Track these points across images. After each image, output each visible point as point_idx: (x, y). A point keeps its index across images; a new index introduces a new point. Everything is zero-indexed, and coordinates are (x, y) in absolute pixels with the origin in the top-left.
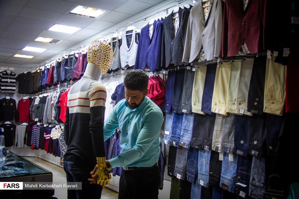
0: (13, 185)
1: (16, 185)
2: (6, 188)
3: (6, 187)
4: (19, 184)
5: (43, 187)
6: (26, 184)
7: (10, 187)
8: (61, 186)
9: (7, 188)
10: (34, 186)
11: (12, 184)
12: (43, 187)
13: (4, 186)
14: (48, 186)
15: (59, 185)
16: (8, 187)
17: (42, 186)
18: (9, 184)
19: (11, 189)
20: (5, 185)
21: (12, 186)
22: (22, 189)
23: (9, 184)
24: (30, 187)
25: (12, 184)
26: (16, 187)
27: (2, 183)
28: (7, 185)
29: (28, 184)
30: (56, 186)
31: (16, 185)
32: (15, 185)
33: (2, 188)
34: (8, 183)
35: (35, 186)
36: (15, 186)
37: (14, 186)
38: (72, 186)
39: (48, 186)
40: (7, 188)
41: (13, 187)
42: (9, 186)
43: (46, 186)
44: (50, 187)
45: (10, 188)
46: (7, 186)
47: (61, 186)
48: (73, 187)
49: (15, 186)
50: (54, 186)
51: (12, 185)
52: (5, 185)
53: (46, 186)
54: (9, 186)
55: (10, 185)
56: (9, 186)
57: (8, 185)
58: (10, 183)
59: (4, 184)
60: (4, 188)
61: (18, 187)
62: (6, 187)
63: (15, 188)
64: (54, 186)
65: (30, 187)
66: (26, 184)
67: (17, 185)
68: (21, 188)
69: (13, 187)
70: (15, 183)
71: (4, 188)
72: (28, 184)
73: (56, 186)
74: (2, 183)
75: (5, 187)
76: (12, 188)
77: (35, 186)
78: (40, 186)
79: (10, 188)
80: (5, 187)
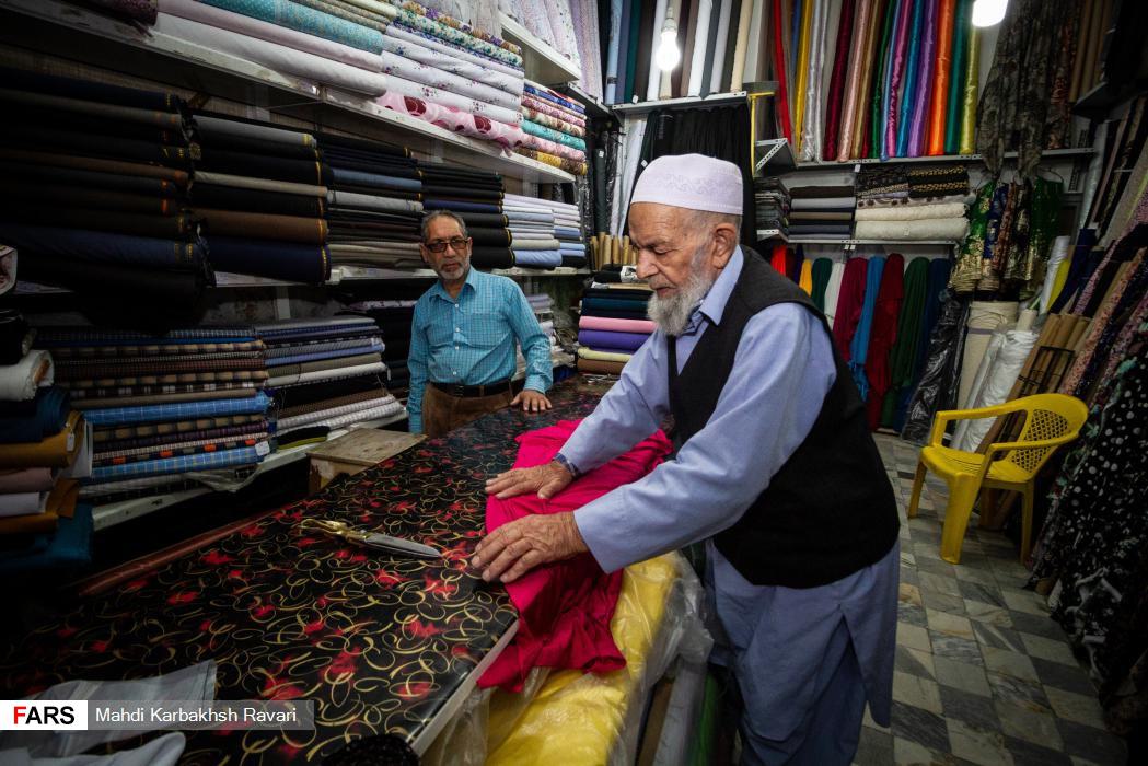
0: (51, 712)
1: (60, 713)
2: (22, 725)
3: (22, 720)
4: (72, 710)
5: (167, 718)
6: (98, 710)
7: (38, 718)
9: (28, 722)
10: (130, 718)
11: (46, 709)
12: (167, 718)
13: (16, 715)
14: (184, 717)
16: (30, 718)
17: (162, 717)
18: (34, 709)
19: (43, 727)
20: (20, 711)
21: (46, 715)
22: (84, 727)
23: (34, 709)
24: (115, 718)
25: (46, 709)
26: (62, 720)
27: (9, 705)
28: (27, 712)
29: (108, 710)
30: (213, 716)
31: (60, 713)
32: (56, 713)
33: (9, 726)
34: (29, 704)
35: (135, 717)
36: (59, 716)
37: (53, 716)
38: (276, 716)
39: (184, 717)
40: (28, 722)
41: (49, 719)
42: (34, 715)
43: (177, 716)
44: (193, 718)
45: (40, 722)
46: (27, 716)
48: (281, 718)
49: (59, 716)
50: (207, 716)
51: (46, 712)
52: (20, 711)
53: (177, 716)
54: (34, 715)
55: (37, 714)
56: (33, 715)
57: (31, 713)
58: (40, 705)
59: (16, 709)
60: (16, 722)
61: (68, 719)
62: (22, 720)
63: (57, 722)
64: (207, 716)
65: (115, 718)
66: (98, 710)
67: (67, 711)
68: (81, 724)
69: (49, 719)
70: (59, 704)
71: (16, 722)
72: (108, 710)
73: (213, 716)
74: (7, 706)
75: (19, 718)
76: (46, 722)
77: (135, 717)
78: (153, 715)
79: (40, 722)
80: (19, 718)
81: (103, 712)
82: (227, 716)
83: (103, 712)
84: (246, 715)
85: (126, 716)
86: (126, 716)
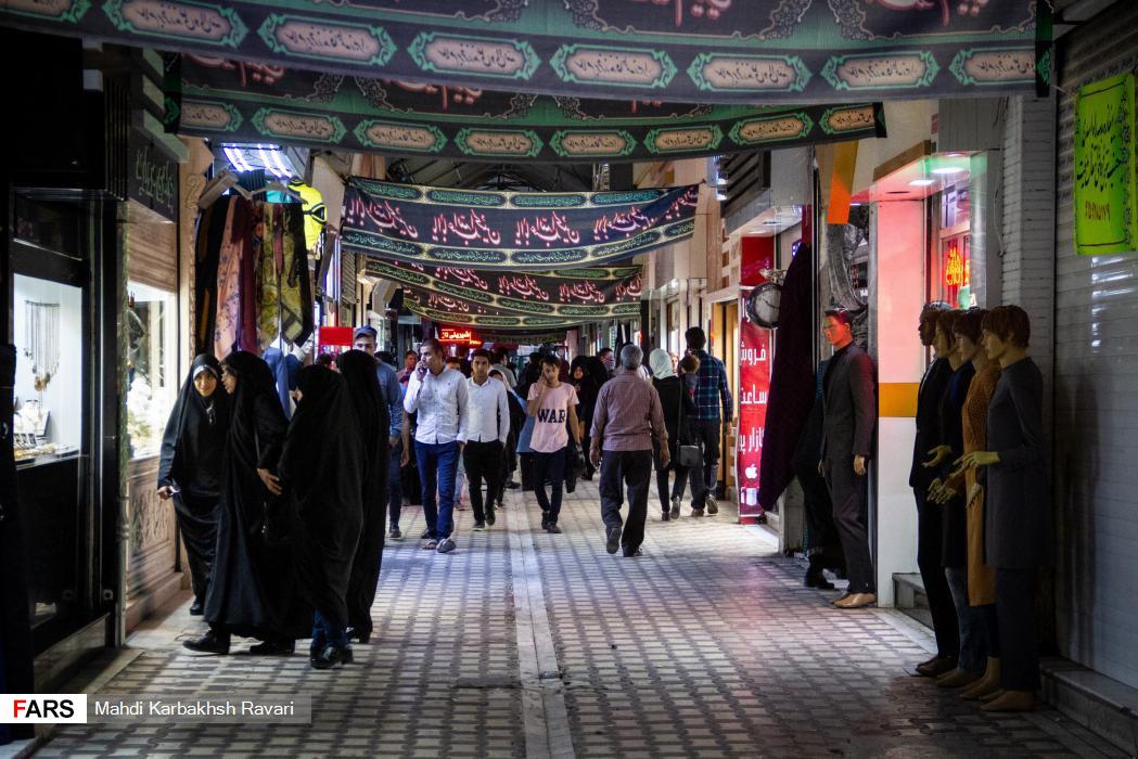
0: (51, 705)
1: (59, 706)
2: (22, 719)
3: (21, 714)
4: (71, 703)
6: (97, 703)
7: (37, 712)
8: (231, 709)
9: (27, 715)
11: (46, 702)
13: (16, 709)
14: (182, 710)
15: (225, 706)
16: (30, 712)
18: (33, 703)
19: (43, 720)
20: (19, 705)
21: (46, 709)
22: (84, 720)
23: (33, 703)
24: (114, 712)
25: (46, 702)
26: (62, 714)
27: (10, 698)
28: (27, 705)
29: (107, 703)
30: (211, 710)
31: (59, 706)
32: (56, 707)
33: (9, 719)
34: (29, 697)
35: (134, 710)
36: (59, 710)
37: (52, 710)
39: (182, 710)
40: (27, 715)
41: (49, 712)
42: (33, 709)
43: (176, 710)
44: (191, 712)
45: (39, 716)
46: (27, 710)
47: (231, 709)
49: (59, 710)
50: (205, 710)
51: (45, 705)
52: (19, 705)
53: (176, 710)
54: (33, 709)
55: (36, 707)
56: (33, 709)
57: (31, 707)
58: (40, 698)
59: (16, 702)
60: (16, 715)
61: (67, 712)
62: (21, 714)
63: (56, 715)
64: (205, 710)
65: (114, 712)
66: (97, 703)
67: (66, 704)
68: (80, 717)
69: (49, 712)
70: (59, 698)
71: (16, 715)
72: (107, 703)
73: (211, 710)
74: (8, 700)
75: (19, 711)
76: (45, 715)
77: (134, 710)
78: (151, 709)
79: (39, 716)
80: (19, 711)
81: (102, 705)
82: (225, 710)
83: (102, 705)
84: (243, 709)
85: (125, 710)
86: (125, 710)
